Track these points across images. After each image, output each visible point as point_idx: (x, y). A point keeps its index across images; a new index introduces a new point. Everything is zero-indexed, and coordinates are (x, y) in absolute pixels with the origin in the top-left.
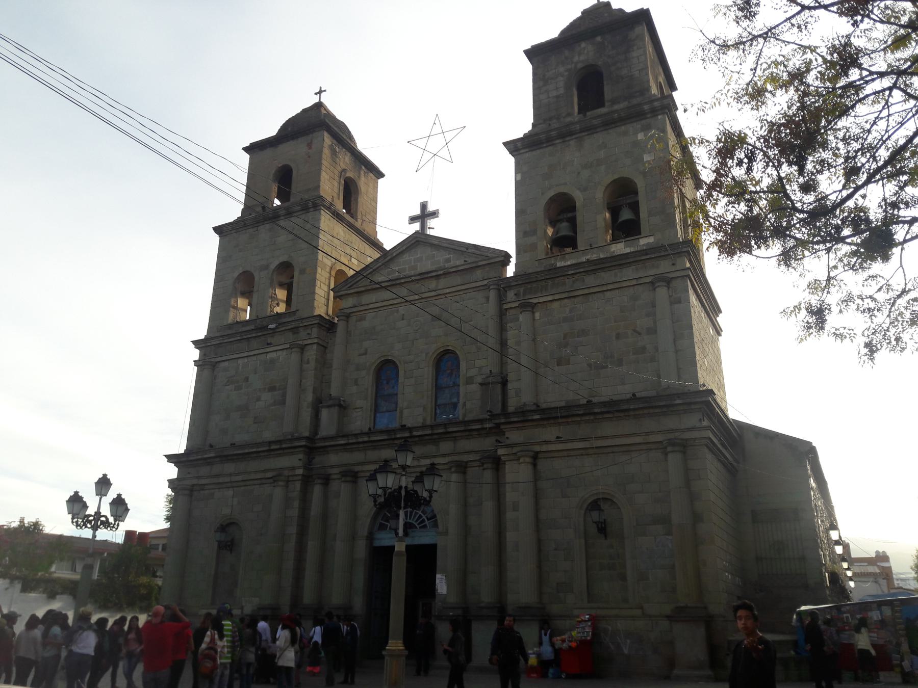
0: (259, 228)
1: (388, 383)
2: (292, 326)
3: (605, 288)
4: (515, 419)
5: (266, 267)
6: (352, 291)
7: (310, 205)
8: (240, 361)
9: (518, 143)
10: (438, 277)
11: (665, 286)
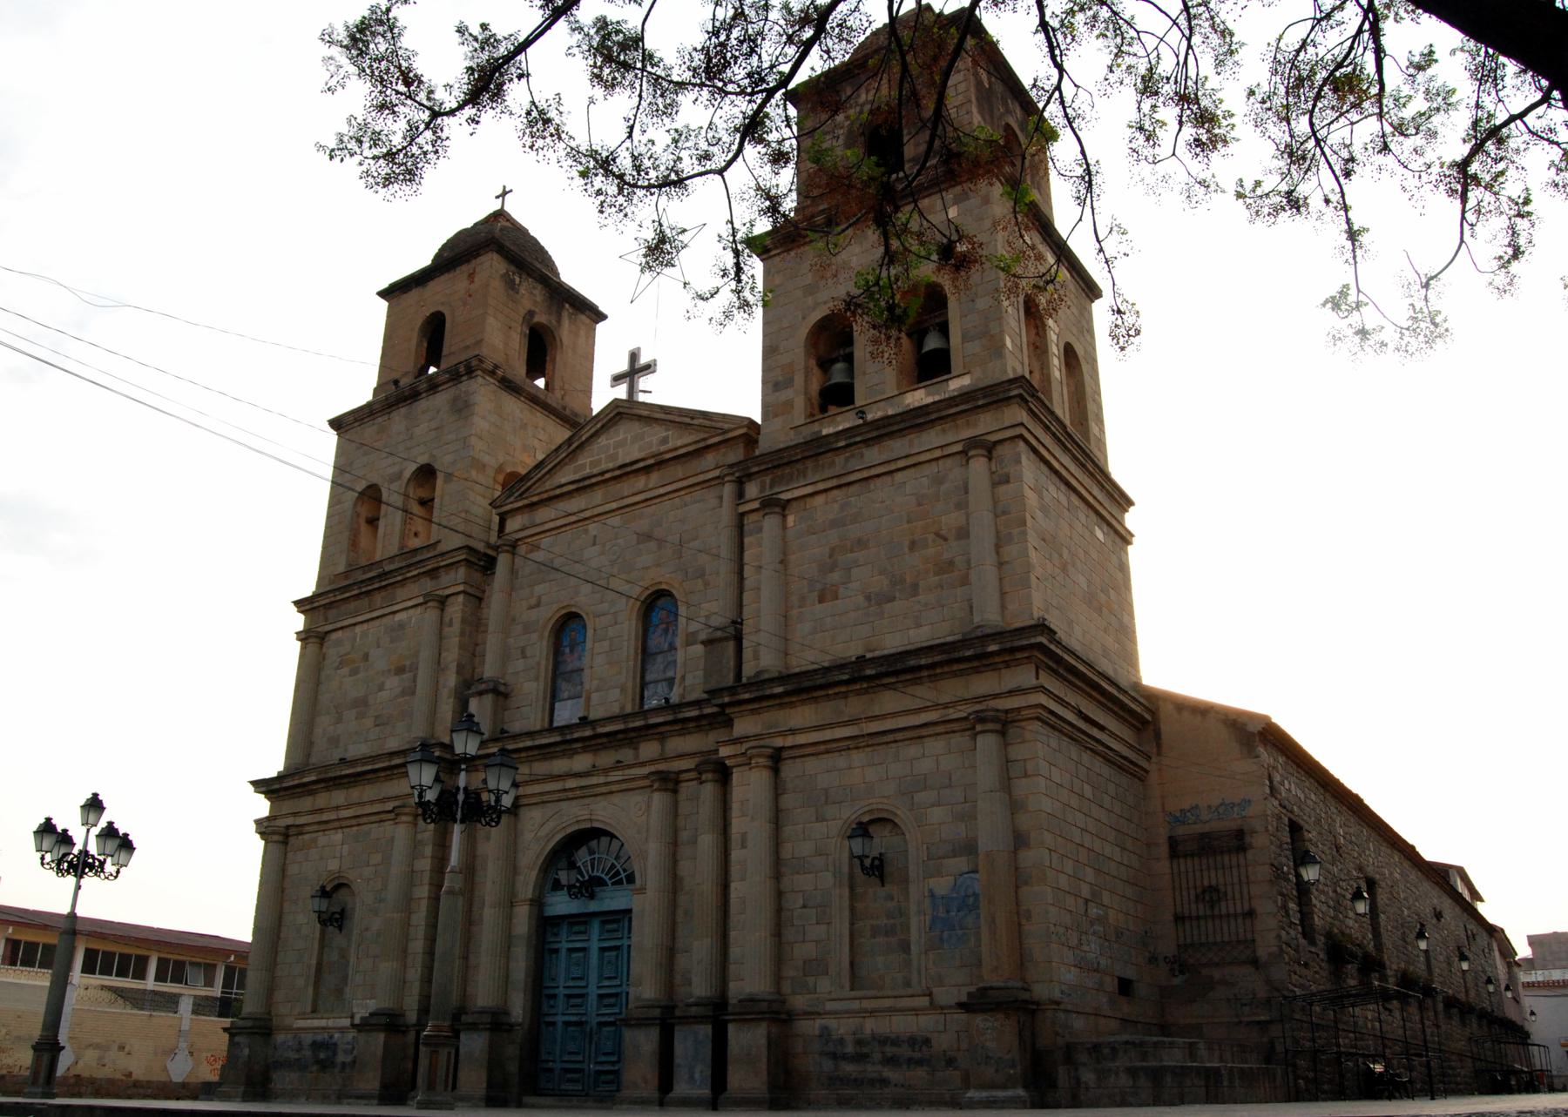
0: (392, 415)
1: (572, 651)
2: (429, 567)
3: (893, 467)
4: (747, 696)
5: (399, 475)
6: (520, 504)
7: (462, 369)
8: (358, 629)
11: (983, 456)
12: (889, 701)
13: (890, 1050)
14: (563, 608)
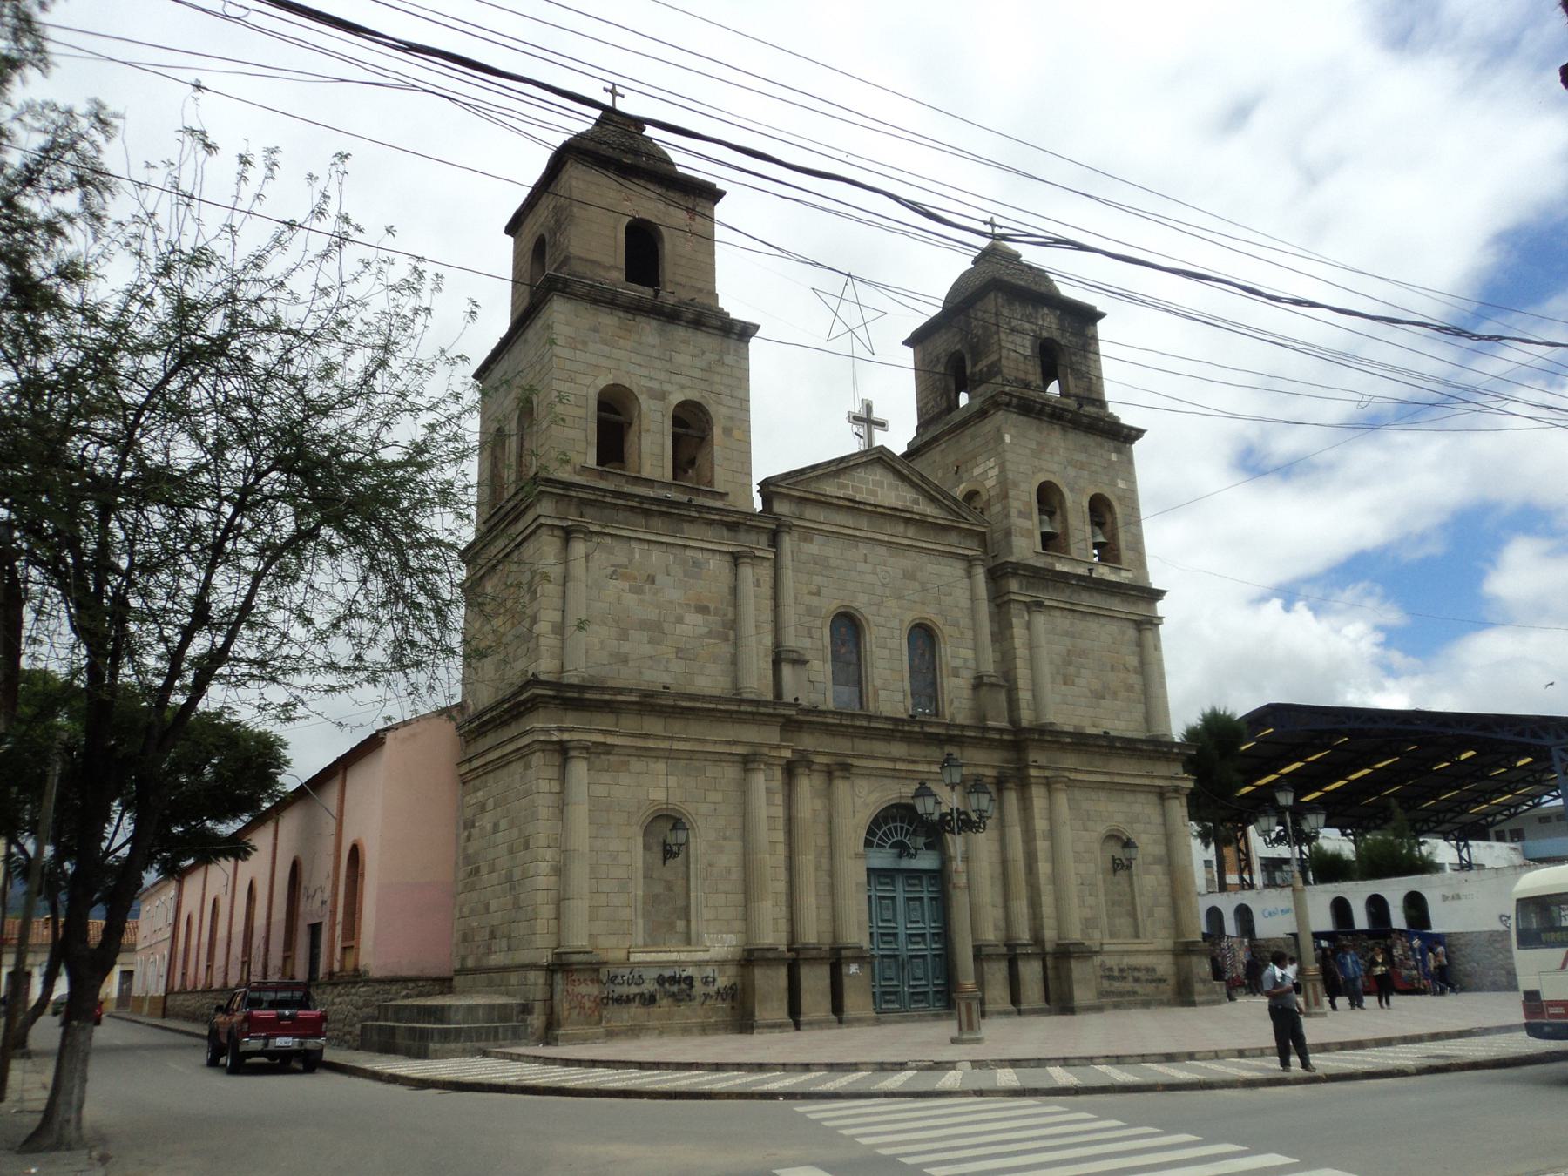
0: (638, 318)
5: (662, 396)
12: (1117, 765)
13: (1136, 974)
14: (844, 606)
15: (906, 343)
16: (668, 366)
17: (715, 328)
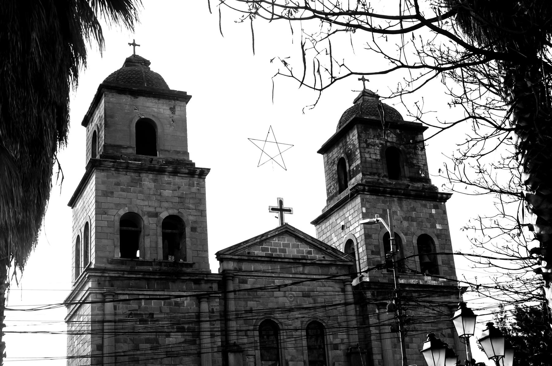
9: (366, 187)
10: (304, 265)
15: (319, 152)
16: (159, 198)
17: (185, 174)
